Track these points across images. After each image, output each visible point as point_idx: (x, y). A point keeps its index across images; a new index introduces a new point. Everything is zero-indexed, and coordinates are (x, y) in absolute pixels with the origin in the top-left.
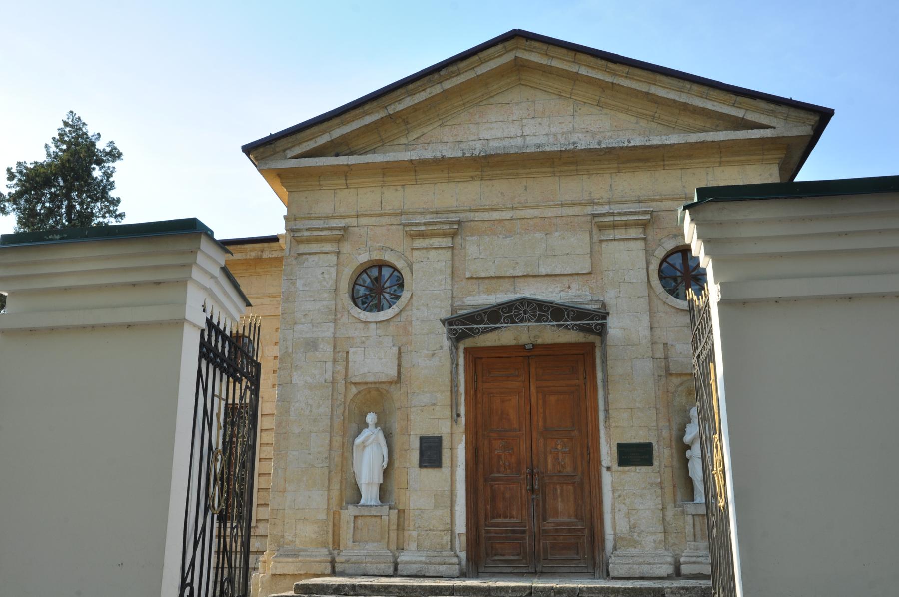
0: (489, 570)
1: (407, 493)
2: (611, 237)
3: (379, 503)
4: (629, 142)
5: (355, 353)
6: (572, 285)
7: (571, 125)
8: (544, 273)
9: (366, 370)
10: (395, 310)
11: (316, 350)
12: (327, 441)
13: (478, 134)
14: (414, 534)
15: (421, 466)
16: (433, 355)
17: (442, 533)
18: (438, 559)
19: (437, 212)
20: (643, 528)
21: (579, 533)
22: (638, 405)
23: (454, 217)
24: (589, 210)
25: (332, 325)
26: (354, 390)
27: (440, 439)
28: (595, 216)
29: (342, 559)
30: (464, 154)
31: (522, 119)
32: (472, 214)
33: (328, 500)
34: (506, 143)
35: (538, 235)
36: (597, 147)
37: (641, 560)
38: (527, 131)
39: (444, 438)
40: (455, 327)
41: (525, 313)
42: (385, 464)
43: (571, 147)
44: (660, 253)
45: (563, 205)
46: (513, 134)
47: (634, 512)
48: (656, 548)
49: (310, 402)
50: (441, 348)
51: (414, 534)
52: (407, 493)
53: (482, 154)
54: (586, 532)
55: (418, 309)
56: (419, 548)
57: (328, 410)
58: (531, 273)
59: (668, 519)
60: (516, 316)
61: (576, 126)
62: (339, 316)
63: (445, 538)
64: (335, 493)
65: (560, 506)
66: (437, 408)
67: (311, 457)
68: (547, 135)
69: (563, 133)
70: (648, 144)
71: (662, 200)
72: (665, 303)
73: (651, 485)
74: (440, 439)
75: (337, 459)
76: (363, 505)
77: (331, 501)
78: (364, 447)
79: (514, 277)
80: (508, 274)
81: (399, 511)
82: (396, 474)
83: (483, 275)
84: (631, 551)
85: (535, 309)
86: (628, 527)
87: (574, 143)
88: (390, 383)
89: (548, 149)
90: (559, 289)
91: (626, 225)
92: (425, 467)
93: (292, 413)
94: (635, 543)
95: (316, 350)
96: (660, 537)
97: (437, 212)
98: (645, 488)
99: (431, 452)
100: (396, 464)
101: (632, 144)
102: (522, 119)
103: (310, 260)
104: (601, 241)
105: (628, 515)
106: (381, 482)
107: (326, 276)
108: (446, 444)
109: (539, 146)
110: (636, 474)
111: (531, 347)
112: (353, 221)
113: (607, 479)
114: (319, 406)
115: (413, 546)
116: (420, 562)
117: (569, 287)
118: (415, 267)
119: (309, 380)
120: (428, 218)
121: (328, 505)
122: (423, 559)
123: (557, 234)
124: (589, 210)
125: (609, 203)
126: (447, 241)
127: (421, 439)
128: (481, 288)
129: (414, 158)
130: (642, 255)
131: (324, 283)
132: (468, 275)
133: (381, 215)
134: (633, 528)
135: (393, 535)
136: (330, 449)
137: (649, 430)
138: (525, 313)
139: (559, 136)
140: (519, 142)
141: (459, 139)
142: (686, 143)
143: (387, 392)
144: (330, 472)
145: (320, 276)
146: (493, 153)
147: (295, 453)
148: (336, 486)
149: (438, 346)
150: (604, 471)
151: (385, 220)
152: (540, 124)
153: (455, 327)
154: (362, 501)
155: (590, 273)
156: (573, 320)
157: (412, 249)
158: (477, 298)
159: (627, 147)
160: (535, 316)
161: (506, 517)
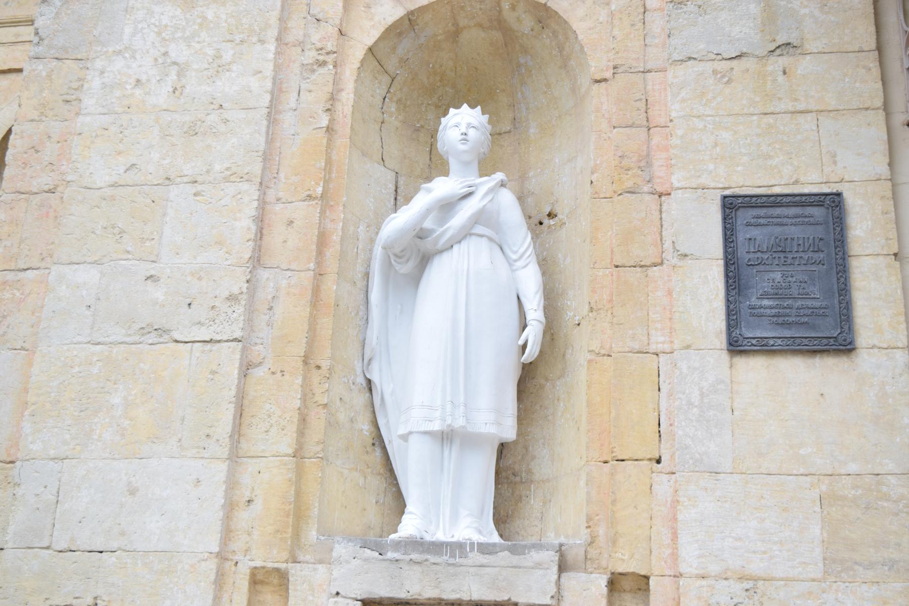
3: (496, 538)
12: (244, 224)
15: (736, 346)
33: (230, 507)
39: (853, 202)
52: (663, 486)
57: (259, 89)
64: (267, 476)
66: (804, 66)
67: (158, 293)
75: (291, 311)
76: (416, 544)
77: (243, 517)
78: (425, 260)
81: (614, 583)
82: (579, 389)
92: (765, 348)
93: (89, 102)
100: (583, 345)
106: (509, 433)
114: (219, 68)
121: (227, 533)
127: (732, 206)
136: (257, 260)
144: (246, 368)
147: (88, 276)
148: (272, 440)
154: (409, 526)
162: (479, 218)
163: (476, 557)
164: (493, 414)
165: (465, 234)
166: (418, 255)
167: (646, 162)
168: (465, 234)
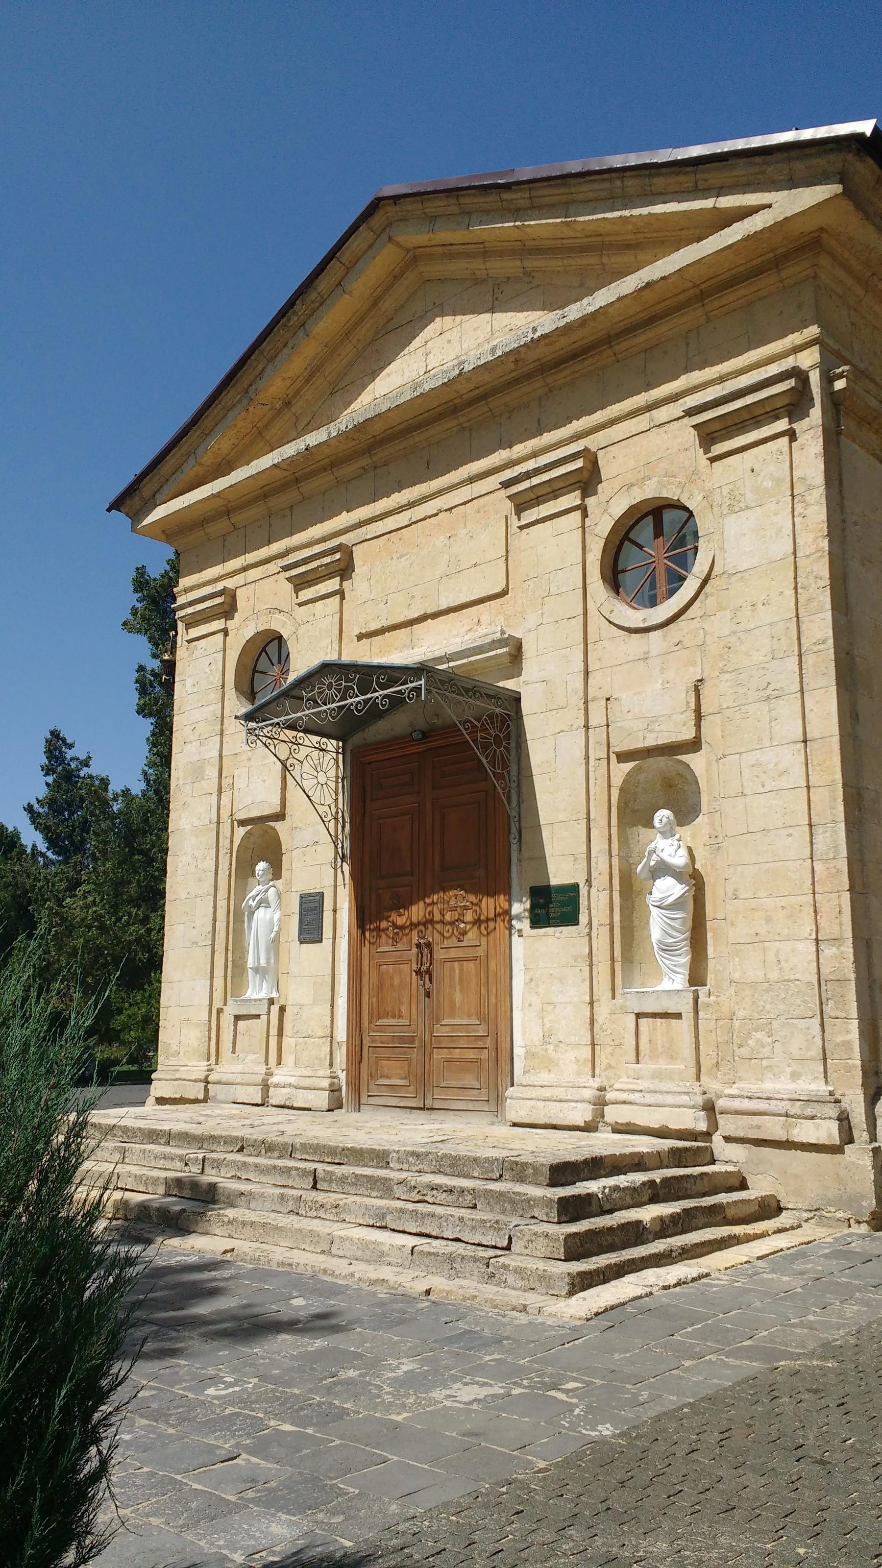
0: (373, 1100)
5: (239, 776)
6: (483, 619)
9: (249, 800)
11: (203, 779)
17: (321, 1041)
20: (561, 1038)
21: (480, 1044)
22: (561, 817)
26: (240, 832)
36: (490, 358)
47: (551, 1007)
48: (579, 1074)
49: (196, 854)
54: (489, 1043)
58: (430, 611)
63: (323, 1048)
65: (458, 997)
67: (195, 932)
80: (402, 619)
83: (374, 626)
88: (280, 816)
89: (427, 387)
90: (466, 628)
95: (203, 779)
103: (199, 648)
107: (213, 667)
110: (555, 938)
112: (239, 579)
119: (196, 822)
122: (292, 1080)
127: (302, 897)
129: (276, 462)
131: (211, 678)
132: (357, 633)
134: (547, 1037)
142: (620, 299)
145: (207, 670)
147: (181, 927)
155: (504, 593)
161: (393, 1017)
163: (253, 1003)
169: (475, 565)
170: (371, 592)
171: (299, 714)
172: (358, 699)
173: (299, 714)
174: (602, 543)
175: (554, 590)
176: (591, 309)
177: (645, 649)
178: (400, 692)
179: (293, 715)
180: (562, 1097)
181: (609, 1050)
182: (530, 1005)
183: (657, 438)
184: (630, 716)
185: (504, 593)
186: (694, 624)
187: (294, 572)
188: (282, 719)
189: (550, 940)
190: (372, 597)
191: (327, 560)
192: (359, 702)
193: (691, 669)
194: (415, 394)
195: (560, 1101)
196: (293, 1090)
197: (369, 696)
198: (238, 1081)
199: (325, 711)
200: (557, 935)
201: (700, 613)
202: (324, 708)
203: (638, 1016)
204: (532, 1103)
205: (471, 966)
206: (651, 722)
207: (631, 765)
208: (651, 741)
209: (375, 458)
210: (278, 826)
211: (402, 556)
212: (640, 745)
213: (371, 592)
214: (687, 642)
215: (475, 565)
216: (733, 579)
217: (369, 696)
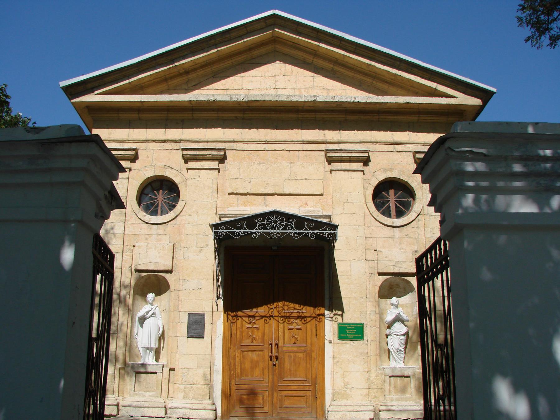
1: (177, 356)
2: (339, 168)
3: (155, 362)
4: (355, 98)
7: (312, 84)
8: (287, 193)
10: (172, 215)
13: (242, 86)
14: (182, 387)
16: (201, 251)
17: (203, 387)
18: (201, 407)
19: (207, 142)
22: (354, 295)
23: (220, 146)
24: (323, 147)
25: (123, 224)
27: (204, 315)
28: (327, 151)
29: (127, 403)
30: (231, 98)
31: (275, 76)
32: (235, 144)
34: (263, 92)
35: (285, 164)
37: (351, 408)
38: (279, 85)
40: (221, 231)
41: (275, 222)
42: (161, 332)
43: (312, 99)
44: (375, 183)
45: (303, 142)
46: (268, 87)
50: (207, 245)
51: (182, 387)
53: (245, 100)
55: (190, 215)
56: (185, 397)
58: (278, 192)
59: (371, 379)
60: (268, 224)
61: (315, 84)
62: (128, 218)
66: (202, 292)
68: (294, 89)
69: (306, 89)
70: (369, 101)
71: (377, 143)
72: (376, 220)
73: (362, 354)
74: (204, 315)
79: (265, 195)
80: (260, 192)
83: (241, 191)
84: (344, 402)
85: (283, 219)
86: (343, 384)
87: (315, 96)
91: (350, 160)
92: (192, 337)
94: (345, 396)
96: (365, 392)
97: (207, 142)
98: (356, 356)
99: (196, 327)
101: (356, 101)
102: (275, 76)
104: (331, 171)
105: (343, 376)
108: (208, 320)
109: (289, 96)
110: (349, 346)
111: (275, 248)
112: (143, 145)
113: (329, 349)
115: (181, 395)
116: (186, 408)
117: (306, 204)
118: (190, 182)
120: (201, 146)
123: (298, 163)
124: (323, 147)
125: (338, 143)
126: (215, 164)
127: (189, 315)
128: (239, 201)
129: (192, 99)
130: (360, 182)
133: (165, 141)
135: (165, 386)
137: (362, 313)
138: (275, 222)
139: (303, 91)
140: (273, 92)
141: (227, 87)
143: (164, 278)
146: (253, 99)
149: (204, 245)
150: (327, 343)
151: (167, 145)
152: (289, 81)
153: (221, 231)
155: (321, 195)
156: (311, 229)
157: (188, 169)
158: (236, 208)
159: (354, 102)
160: (282, 225)
162: (153, 314)
164: (154, 344)
165: (151, 316)
166: (142, 320)
167: (178, 306)
168: (151, 316)
169: (306, 179)
170: (240, 175)
171: (253, 231)
172: (295, 231)
173: (253, 231)
174: (373, 188)
175: (350, 201)
176: (383, 101)
177: (393, 234)
178: (323, 233)
179: (249, 231)
180: (359, 410)
181: (375, 390)
182: (337, 372)
183: (396, 156)
184: (387, 259)
185: (321, 195)
186: (414, 230)
187: (185, 153)
188: (241, 231)
189: (348, 346)
190: (240, 177)
191: (215, 153)
192: (296, 233)
193: (413, 246)
194: (288, 100)
195: (357, 411)
196: (189, 410)
197: (302, 231)
198: (145, 406)
199: (272, 233)
200: (352, 344)
201: (416, 226)
202: (272, 231)
203: (390, 377)
204: (343, 412)
205: (301, 355)
206: (397, 263)
207: (385, 278)
208: (396, 270)
209: (245, 116)
210: (167, 276)
211: (260, 163)
212: (392, 271)
213: (240, 175)
214: (411, 235)
215: (306, 179)
216: (431, 217)
217: (302, 231)
